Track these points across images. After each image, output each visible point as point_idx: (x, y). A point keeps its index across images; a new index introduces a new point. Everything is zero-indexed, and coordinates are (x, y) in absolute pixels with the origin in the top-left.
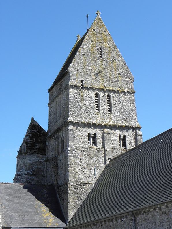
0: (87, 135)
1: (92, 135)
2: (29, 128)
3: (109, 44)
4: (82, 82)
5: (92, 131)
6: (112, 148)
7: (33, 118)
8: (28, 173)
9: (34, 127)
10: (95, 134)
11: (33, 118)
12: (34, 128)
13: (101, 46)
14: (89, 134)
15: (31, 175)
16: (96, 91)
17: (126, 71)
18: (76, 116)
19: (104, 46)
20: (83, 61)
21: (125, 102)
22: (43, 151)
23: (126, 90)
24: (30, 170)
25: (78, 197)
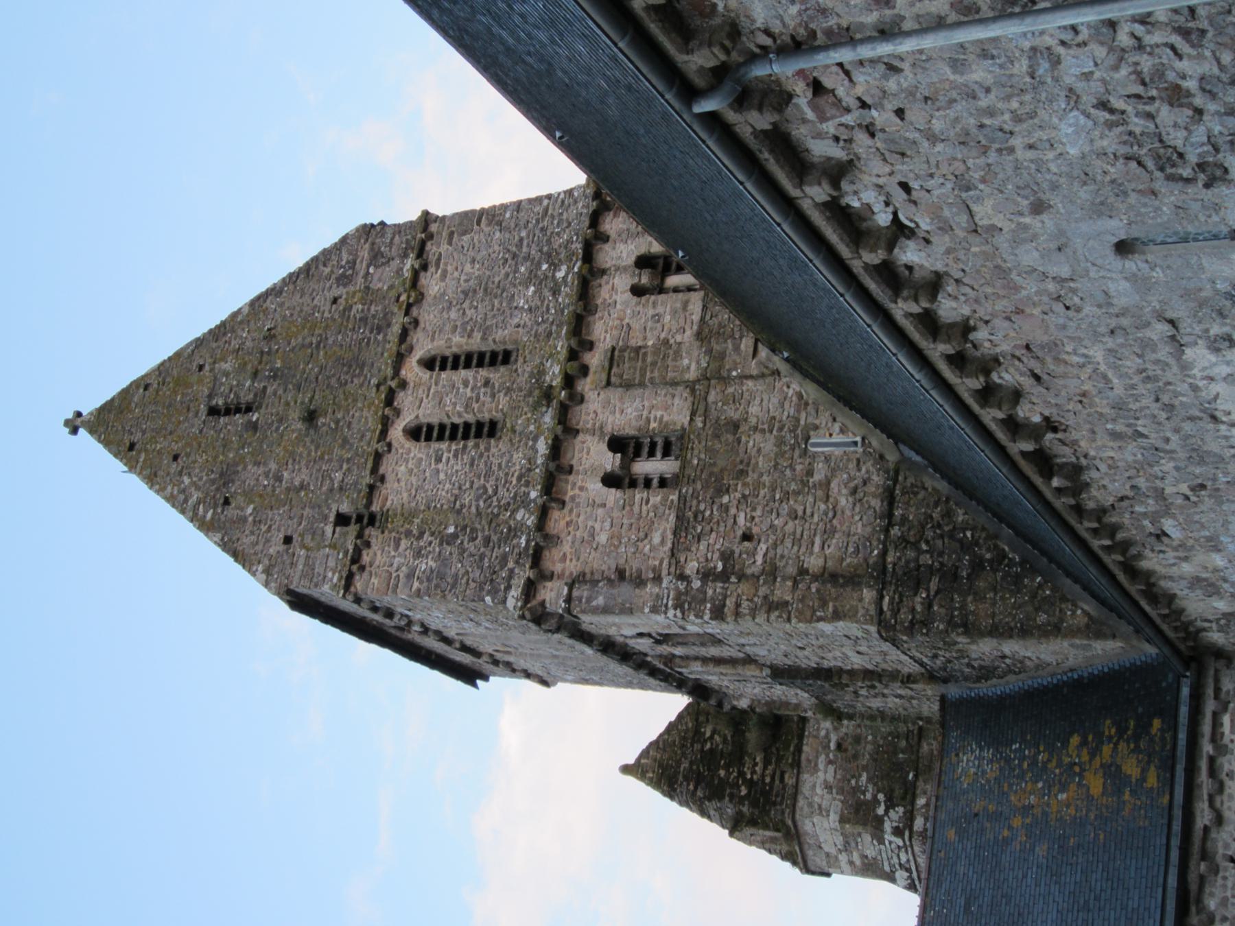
0: (613, 495)
1: (610, 461)
2: (672, 798)
3: (201, 368)
4: (342, 520)
5: (593, 456)
6: (699, 335)
7: (626, 769)
8: (898, 832)
9: (676, 768)
10: (617, 444)
11: (626, 769)
12: (676, 768)
13: (203, 408)
14: (610, 480)
15: (909, 818)
16: (396, 433)
17: (327, 270)
18: (504, 559)
19: (206, 392)
20: (249, 510)
21: (468, 268)
22: (780, 730)
23: (410, 263)
24: (879, 821)
25: (977, 566)
